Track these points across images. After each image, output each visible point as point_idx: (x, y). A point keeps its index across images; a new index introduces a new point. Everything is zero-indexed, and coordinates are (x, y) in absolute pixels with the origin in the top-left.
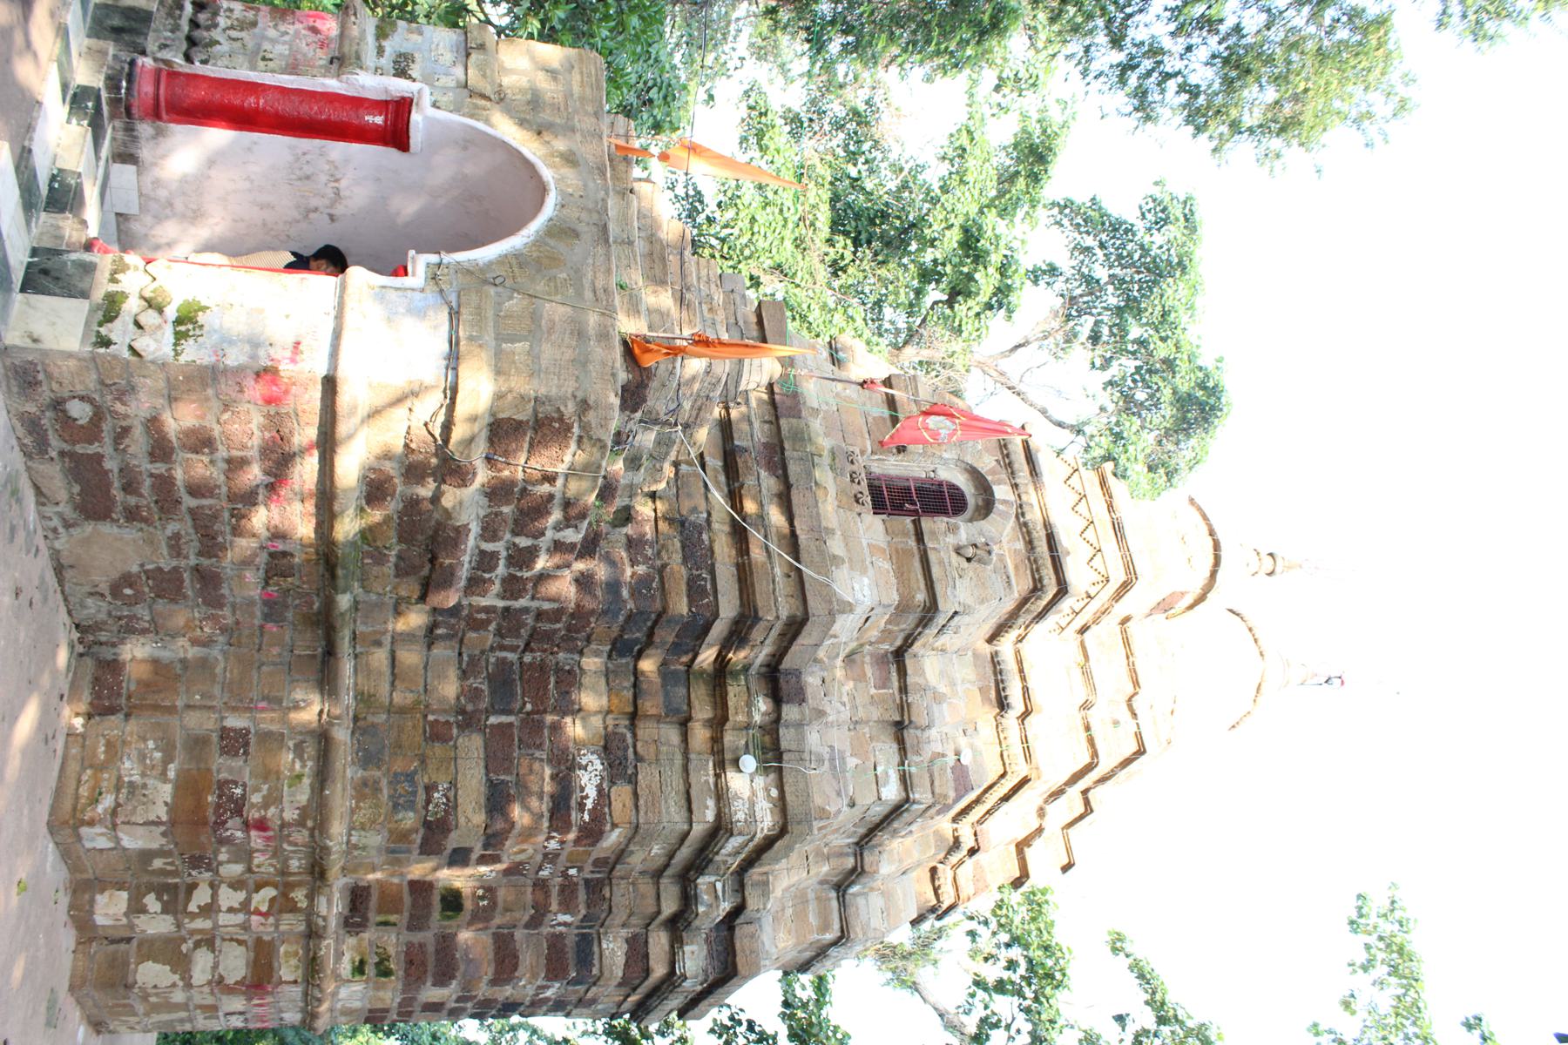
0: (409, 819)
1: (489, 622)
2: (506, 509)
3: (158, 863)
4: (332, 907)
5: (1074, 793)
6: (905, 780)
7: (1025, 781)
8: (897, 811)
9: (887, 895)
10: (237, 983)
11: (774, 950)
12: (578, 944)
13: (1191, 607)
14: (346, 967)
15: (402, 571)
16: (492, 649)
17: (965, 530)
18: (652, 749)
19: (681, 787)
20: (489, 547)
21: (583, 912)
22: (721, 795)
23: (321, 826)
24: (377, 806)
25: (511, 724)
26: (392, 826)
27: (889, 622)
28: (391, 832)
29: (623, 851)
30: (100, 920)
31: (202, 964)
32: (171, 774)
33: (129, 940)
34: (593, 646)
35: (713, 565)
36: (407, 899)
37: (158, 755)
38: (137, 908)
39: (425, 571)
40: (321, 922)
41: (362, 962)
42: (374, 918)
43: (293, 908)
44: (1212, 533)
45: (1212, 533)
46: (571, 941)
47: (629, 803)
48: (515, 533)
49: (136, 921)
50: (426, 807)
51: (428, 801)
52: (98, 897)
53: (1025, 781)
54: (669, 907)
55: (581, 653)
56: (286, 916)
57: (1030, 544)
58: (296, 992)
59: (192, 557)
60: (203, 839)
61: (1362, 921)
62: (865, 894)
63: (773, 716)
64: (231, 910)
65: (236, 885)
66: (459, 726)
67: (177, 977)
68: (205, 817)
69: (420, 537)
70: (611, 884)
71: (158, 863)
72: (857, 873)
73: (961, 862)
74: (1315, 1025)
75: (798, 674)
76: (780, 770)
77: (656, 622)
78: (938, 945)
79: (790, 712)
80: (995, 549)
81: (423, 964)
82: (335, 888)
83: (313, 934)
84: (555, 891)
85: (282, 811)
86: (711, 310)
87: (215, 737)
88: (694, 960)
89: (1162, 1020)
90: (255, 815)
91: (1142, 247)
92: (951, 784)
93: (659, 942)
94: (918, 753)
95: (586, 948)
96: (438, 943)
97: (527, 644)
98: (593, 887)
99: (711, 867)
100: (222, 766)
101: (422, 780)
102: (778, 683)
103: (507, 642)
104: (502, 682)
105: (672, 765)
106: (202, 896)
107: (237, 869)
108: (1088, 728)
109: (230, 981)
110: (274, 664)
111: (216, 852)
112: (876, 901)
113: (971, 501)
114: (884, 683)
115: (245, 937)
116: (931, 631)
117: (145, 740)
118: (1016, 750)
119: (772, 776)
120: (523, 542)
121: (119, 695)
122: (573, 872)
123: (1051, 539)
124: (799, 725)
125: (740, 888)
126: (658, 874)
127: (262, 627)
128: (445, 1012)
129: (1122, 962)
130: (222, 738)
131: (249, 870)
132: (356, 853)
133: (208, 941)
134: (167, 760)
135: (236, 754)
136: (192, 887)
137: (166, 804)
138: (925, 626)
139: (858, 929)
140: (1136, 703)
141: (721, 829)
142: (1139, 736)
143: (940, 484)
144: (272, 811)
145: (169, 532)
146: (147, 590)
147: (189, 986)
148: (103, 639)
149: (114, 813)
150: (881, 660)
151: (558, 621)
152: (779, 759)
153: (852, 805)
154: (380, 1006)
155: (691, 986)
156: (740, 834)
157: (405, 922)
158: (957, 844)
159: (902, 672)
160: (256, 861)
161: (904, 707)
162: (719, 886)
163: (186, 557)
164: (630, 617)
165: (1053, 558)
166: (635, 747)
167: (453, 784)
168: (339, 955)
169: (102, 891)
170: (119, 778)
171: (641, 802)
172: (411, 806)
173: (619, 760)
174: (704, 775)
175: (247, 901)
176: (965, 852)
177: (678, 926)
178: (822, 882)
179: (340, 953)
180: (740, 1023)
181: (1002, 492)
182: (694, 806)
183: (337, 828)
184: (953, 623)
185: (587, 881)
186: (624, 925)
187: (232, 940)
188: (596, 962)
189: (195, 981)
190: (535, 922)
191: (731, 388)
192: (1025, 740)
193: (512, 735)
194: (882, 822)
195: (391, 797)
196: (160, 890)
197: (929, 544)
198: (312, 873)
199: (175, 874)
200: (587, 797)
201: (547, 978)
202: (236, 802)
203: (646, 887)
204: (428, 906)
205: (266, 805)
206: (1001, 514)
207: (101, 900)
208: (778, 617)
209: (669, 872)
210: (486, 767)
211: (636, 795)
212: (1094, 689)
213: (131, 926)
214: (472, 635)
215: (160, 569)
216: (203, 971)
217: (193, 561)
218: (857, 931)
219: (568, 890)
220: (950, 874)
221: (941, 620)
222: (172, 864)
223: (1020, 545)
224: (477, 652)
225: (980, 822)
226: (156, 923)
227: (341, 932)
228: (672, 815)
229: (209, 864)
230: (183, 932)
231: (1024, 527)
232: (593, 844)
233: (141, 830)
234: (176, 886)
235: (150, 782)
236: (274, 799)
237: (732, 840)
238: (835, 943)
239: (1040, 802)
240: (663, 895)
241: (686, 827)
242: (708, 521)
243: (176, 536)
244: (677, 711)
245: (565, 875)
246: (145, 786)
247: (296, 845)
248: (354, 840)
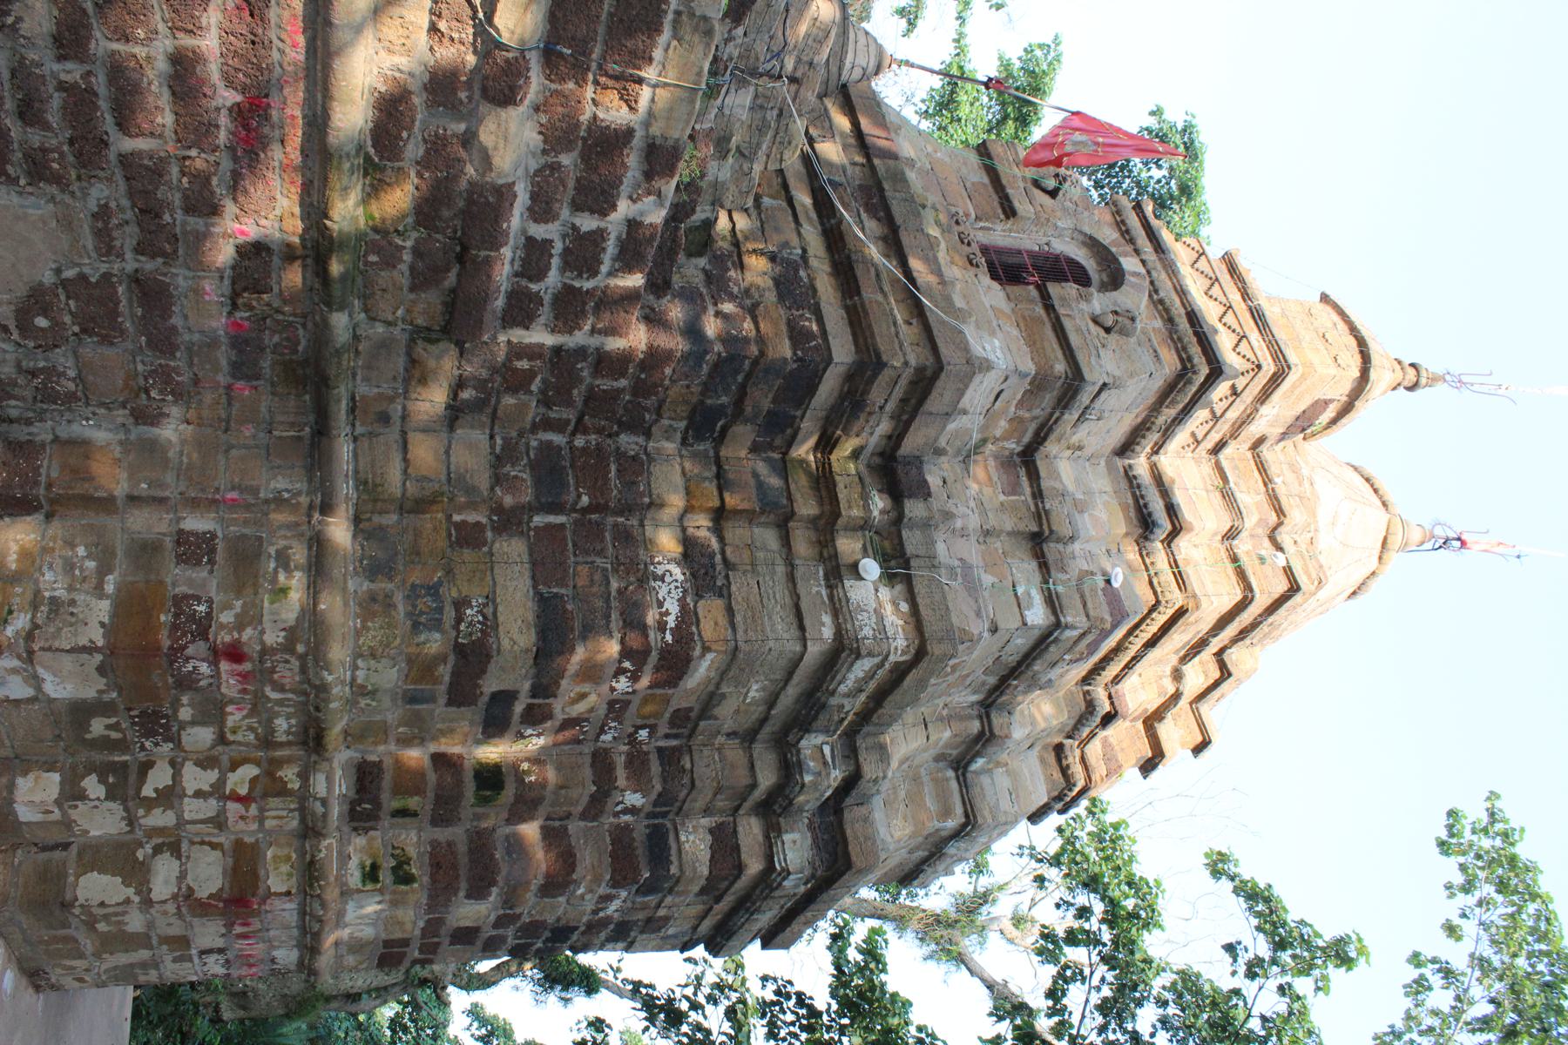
0: (434, 643)
1: (530, 375)
2: (566, 160)
3: (98, 727)
4: (333, 784)
5: (1207, 655)
6: (1052, 601)
7: (1180, 613)
8: (1043, 642)
9: (1013, 775)
10: (211, 896)
11: (889, 839)
12: (650, 837)
13: (1334, 421)
14: (354, 878)
15: (420, 281)
16: (535, 428)
17: (1099, 302)
18: (746, 554)
19: (788, 600)
20: (539, 231)
21: (658, 787)
22: (838, 608)
23: (315, 657)
24: (390, 626)
25: (562, 525)
26: (412, 650)
27: (1020, 404)
28: (410, 661)
29: (712, 695)
30: (25, 814)
31: (164, 877)
32: (110, 588)
33: (66, 846)
34: (666, 422)
35: (817, 305)
36: (432, 777)
37: (91, 565)
38: (72, 793)
39: (451, 279)
40: (319, 809)
41: (375, 867)
42: (391, 803)
43: (282, 791)
46: (640, 831)
47: (723, 621)
48: (577, 207)
49: (74, 814)
50: (456, 627)
51: (459, 620)
52: (20, 781)
53: (1180, 613)
54: (767, 778)
55: (648, 435)
56: (274, 802)
57: (1170, 320)
58: (287, 911)
59: (129, 255)
60: (155, 677)
61: (1454, 841)
62: (989, 771)
63: (893, 515)
64: (198, 794)
65: (205, 763)
66: (493, 529)
67: (130, 891)
68: (157, 641)
69: (446, 213)
70: (691, 752)
71: (98, 727)
72: (985, 739)
73: (1092, 735)
74: (1416, 955)
75: (917, 462)
76: (908, 580)
77: (748, 376)
78: (984, 910)
79: (914, 509)
81: (454, 867)
82: (336, 764)
83: (310, 830)
84: (620, 761)
85: (263, 632)
87: (168, 543)
88: (796, 849)
89: (1280, 945)
90: (225, 638)
91: (1138, 183)
92: (1105, 607)
93: (750, 831)
94: (1063, 570)
95: (659, 844)
96: (471, 841)
97: (580, 420)
98: (669, 757)
99: (822, 720)
100: (179, 578)
101: (451, 593)
102: (895, 473)
103: (556, 413)
104: (548, 469)
105: (774, 573)
106: (159, 777)
107: (200, 737)
108: (1235, 559)
109: (203, 893)
110: (247, 447)
111: (176, 705)
112: (1002, 780)
114: (1014, 489)
115: (221, 839)
116: (1071, 416)
117: (72, 546)
118: (1167, 577)
119: (899, 587)
120: (587, 223)
121: (37, 483)
122: (643, 734)
123: (1193, 317)
124: (926, 525)
125: (851, 751)
126: (748, 737)
127: (229, 387)
128: (479, 943)
129: (1226, 885)
130: (178, 543)
131: (222, 739)
132: (363, 702)
133: (171, 844)
134: (103, 570)
135: (199, 563)
136: (147, 766)
137: (102, 624)
138: (1065, 407)
139: (986, 813)
140: (1284, 537)
141: (843, 649)
142: (1288, 571)
143: (1057, 258)
144: (248, 633)
145: (93, 206)
146: (67, 319)
147: (147, 903)
148: (14, 413)
149: (29, 636)
150: (1006, 463)
151: (623, 374)
152: (907, 564)
153: (994, 630)
154: (398, 935)
155: (794, 885)
156: (870, 654)
157: (429, 807)
158: (1091, 706)
159: (1034, 475)
160: (230, 721)
161: (1041, 515)
162: (827, 750)
163: (121, 256)
164: (716, 366)
165: (1196, 334)
166: (723, 552)
167: (491, 599)
168: (344, 858)
169: (25, 773)
170: (37, 593)
171: (738, 618)
172: (437, 625)
173: (704, 570)
174: (814, 588)
175: (222, 782)
176: (1098, 720)
177: (774, 809)
178: (938, 759)
179: (343, 854)
180: (788, 997)
182: (807, 622)
183: (338, 652)
184: (1098, 404)
185: (660, 750)
186: (707, 811)
187: (203, 843)
188: (674, 858)
189: (155, 896)
190: (596, 805)
191: (834, 69)
192: (1174, 564)
193: (564, 539)
194: (1020, 663)
195: (409, 615)
196: (102, 772)
197: (1062, 311)
198: (304, 743)
199: (122, 745)
200: (667, 613)
201: (616, 883)
202: (199, 622)
203: (735, 753)
204: (459, 783)
205: (240, 626)
206: (1133, 286)
207: (24, 784)
208: (906, 363)
209: (767, 729)
210: (533, 578)
211: (730, 611)
213: (67, 824)
214: (509, 400)
215: (83, 277)
216: (166, 882)
217: (130, 266)
218: (984, 815)
219: (637, 762)
220: (1077, 752)
221: (1084, 398)
222: (115, 727)
223: (1158, 323)
224: (514, 434)
225: (1117, 679)
226: (101, 820)
227: (346, 829)
228: (779, 633)
229: (167, 727)
230: (139, 834)
231: (1159, 304)
232: (675, 686)
233: (67, 662)
234: (125, 764)
235: (80, 598)
236: (250, 617)
237: (859, 663)
238: (957, 834)
239: (1174, 660)
240: (758, 764)
241: (798, 648)
242: (804, 256)
243: (103, 213)
244: (776, 505)
245: (632, 739)
246: (73, 602)
247: (282, 689)
248: (360, 674)
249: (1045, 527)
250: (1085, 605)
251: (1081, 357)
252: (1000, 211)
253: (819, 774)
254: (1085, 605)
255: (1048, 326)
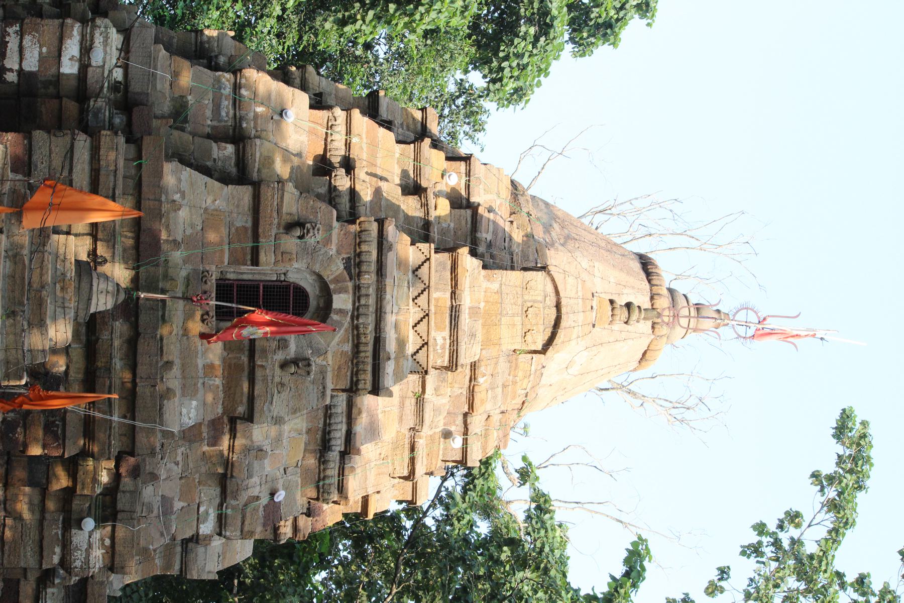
6: (222, 521)
19: (37, 537)
22: (66, 545)
44: (558, 306)
45: (558, 306)
80: (317, 362)
86: (62, 289)
94: (235, 498)
108: (413, 449)
113: (313, 303)
123: (378, 341)
124: (136, 493)
171: (6, 548)
181: (342, 301)
182: (45, 554)
197: (259, 362)
212: (421, 421)
223: (348, 347)
249: (229, 472)
250: (243, 523)
251: (258, 404)
252: (249, 257)
253: (65, 578)
254: (243, 523)
255: (246, 373)
